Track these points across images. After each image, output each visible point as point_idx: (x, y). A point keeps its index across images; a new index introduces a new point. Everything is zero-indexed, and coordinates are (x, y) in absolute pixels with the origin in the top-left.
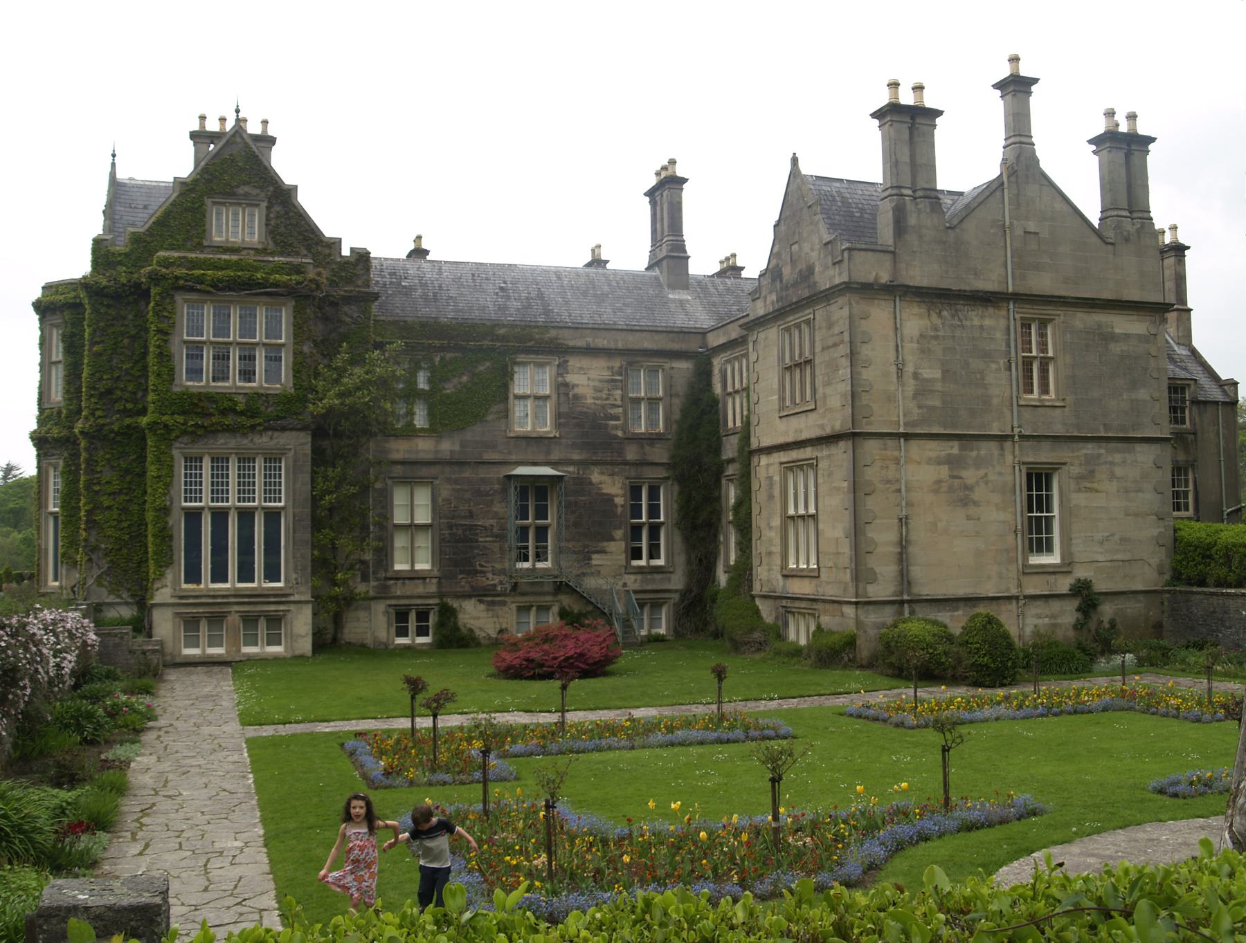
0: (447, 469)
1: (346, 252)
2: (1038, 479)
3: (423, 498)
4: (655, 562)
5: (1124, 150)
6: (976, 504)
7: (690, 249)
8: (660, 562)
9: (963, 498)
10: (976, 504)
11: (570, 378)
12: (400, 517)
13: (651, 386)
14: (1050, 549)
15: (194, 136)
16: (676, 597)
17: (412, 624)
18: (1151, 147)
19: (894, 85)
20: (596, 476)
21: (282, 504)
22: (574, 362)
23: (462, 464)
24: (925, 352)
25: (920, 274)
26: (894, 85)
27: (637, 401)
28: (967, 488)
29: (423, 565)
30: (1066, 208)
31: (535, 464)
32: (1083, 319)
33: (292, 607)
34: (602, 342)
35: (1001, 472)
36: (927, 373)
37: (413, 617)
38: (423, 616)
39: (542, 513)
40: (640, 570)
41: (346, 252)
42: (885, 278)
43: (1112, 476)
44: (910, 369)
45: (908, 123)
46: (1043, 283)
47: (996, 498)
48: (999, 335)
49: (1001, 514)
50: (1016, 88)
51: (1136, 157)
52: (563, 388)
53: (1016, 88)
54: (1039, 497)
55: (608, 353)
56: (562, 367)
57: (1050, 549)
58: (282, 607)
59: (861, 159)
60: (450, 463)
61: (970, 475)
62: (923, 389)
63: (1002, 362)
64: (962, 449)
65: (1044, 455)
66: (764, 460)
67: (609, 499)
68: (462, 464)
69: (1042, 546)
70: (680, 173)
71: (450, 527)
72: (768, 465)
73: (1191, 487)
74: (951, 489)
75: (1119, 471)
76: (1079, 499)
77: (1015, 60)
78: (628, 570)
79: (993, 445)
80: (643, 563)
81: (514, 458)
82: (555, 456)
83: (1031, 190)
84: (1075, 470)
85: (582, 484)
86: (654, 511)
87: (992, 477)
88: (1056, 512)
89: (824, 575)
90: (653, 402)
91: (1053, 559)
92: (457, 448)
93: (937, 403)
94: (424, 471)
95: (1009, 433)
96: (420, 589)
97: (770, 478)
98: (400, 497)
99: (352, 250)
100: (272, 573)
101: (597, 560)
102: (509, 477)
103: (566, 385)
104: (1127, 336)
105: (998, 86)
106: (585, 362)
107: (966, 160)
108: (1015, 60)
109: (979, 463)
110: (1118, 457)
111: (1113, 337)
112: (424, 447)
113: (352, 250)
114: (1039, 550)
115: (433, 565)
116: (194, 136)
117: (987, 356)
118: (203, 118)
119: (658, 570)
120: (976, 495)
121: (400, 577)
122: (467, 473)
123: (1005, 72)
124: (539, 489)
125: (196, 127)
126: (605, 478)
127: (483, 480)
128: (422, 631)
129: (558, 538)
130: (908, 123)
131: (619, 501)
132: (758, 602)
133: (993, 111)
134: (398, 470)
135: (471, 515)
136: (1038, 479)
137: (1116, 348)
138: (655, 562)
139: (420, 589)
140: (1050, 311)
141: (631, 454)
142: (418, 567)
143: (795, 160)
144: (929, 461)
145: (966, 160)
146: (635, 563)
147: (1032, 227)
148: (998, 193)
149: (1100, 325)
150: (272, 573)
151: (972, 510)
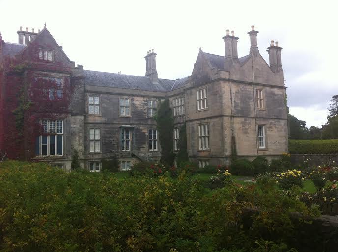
0: (104, 125)
1: (76, 66)
2: (260, 127)
3: (98, 132)
4: (155, 150)
5: (274, 50)
6: (248, 133)
7: (158, 71)
8: (156, 150)
9: (246, 133)
10: (248, 133)
11: (134, 102)
12: (92, 138)
13: (154, 105)
14: (263, 145)
15: (18, 32)
16: (160, 158)
17: (94, 167)
18: (282, 50)
19: (228, 31)
20: (141, 127)
21: (63, 133)
22: (136, 98)
23: (109, 124)
24: (236, 96)
25: (235, 77)
26: (228, 31)
27: (150, 108)
28: (246, 129)
29: (98, 151)
30: (264, 63)
31: (126, 124)
32: (269, 89)
33: (66, 162)
34: (142, 93)
35: (253, 125)
36: (237, 101)
37: (95, 165)
38: (97, 164)
39: (128, 137)
40: (152, 152)
41: (76, 66)
42: (228, 78)
43: (276, 128)
44: (233, 100)
45: (231, 40)
46: (260, 81)
47: (252, 132)
48: (252, 93)
49: (252, 136)
50: (253, 34)
51: (278, 53)
52: (132, 105)
53: (253, 34)
54: (260, 132)
55: (144, 96)
56: (133, 100)
57: (263, 145)
58: (63, 162)
59: (220, 50)
60: (105, 123)
61: (247, 127)
62: (236, 105)
63: (253, 99)
64: (245, 120)
65: (263, 122)
66: (190, 123)
67: (144, 134)
68: (109, 124)
69: (261, 144)
70: (155, 52)
71: (105, 140)
72: (192, 124)
73: (264, 136)
74: (243, 130)
75: (277, 127)
76: (269, 133)
77: (253, 27)
78: (149, 151)
79: (251, 119)
80: (152, 150)
81: (121, 122)
82: (131, 122)
83: (257, 59)
84: (268, 126)
85: (138, 130)
86: (155, 137)
87: (251, 127)
88: (264, 136)
89: (212, 150)
90: (154, 109)
91: (264, 147)
92: (106, 120)
93: (239, 109)
94: (97, 126)
95: (254, 116)
96: (97, 157)
97: (193, 128)
98: (92, 132)
99: (78, 65)
100: (60, 152)
101: (142, 149)
102: (120, 127)
103: (134, 104)
104: (278, 94)
105: (249, 33)
106: (138, 98)
107: (243, 50)
108: (253, 27)
109: (249, 123)
110: (277, 123)
111: (274, 94)
112: (98, 120)
113: (78, 65)
114: (261, 145)
115: (100, 150)
116: (18, 32)
117: (249, 98)
118: (21, 28)
119: (156, 152)
120: (248, 132)
121: (91, 154)
122: (109, 126)
123: (250, 30)
124: (127, 130)
125: (19, 30)
126: (143, 128)
127: (114, 129)
128: (97, 169)
129: (132, 143)
130: (231, 40)
131: (147, 134)
132: (189, 159)
133: (248, 39)
134: (91, 125)
135: (110, 137)
136: (260, 127)
137: (276, 97)
138: (155, 150)
139: (97, 157)
140: (262, 87)
141: (149, 122)
142: (96, 151)
143: (200, 49)
144: (238, 123)
145: (243, 50)
146: (150, 150)
147: (258, 68)
148: (251, 59)
149: (272, 92)
150: (60, 152)
151: (248, 135)
